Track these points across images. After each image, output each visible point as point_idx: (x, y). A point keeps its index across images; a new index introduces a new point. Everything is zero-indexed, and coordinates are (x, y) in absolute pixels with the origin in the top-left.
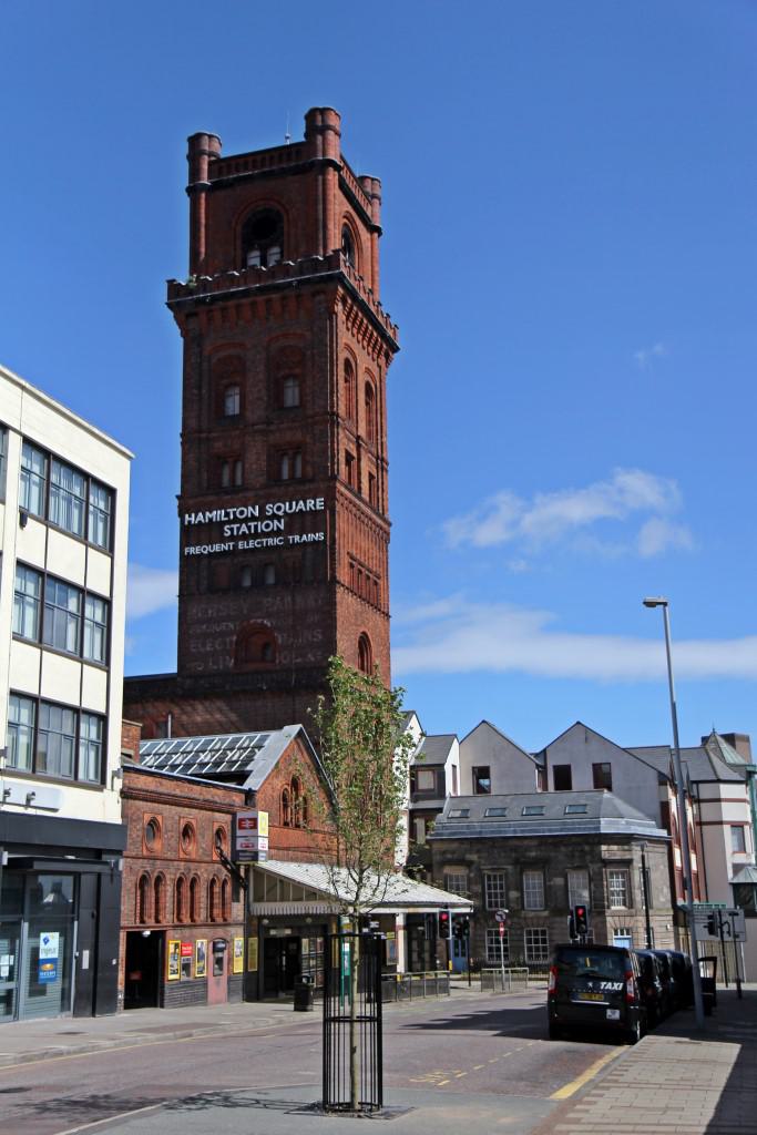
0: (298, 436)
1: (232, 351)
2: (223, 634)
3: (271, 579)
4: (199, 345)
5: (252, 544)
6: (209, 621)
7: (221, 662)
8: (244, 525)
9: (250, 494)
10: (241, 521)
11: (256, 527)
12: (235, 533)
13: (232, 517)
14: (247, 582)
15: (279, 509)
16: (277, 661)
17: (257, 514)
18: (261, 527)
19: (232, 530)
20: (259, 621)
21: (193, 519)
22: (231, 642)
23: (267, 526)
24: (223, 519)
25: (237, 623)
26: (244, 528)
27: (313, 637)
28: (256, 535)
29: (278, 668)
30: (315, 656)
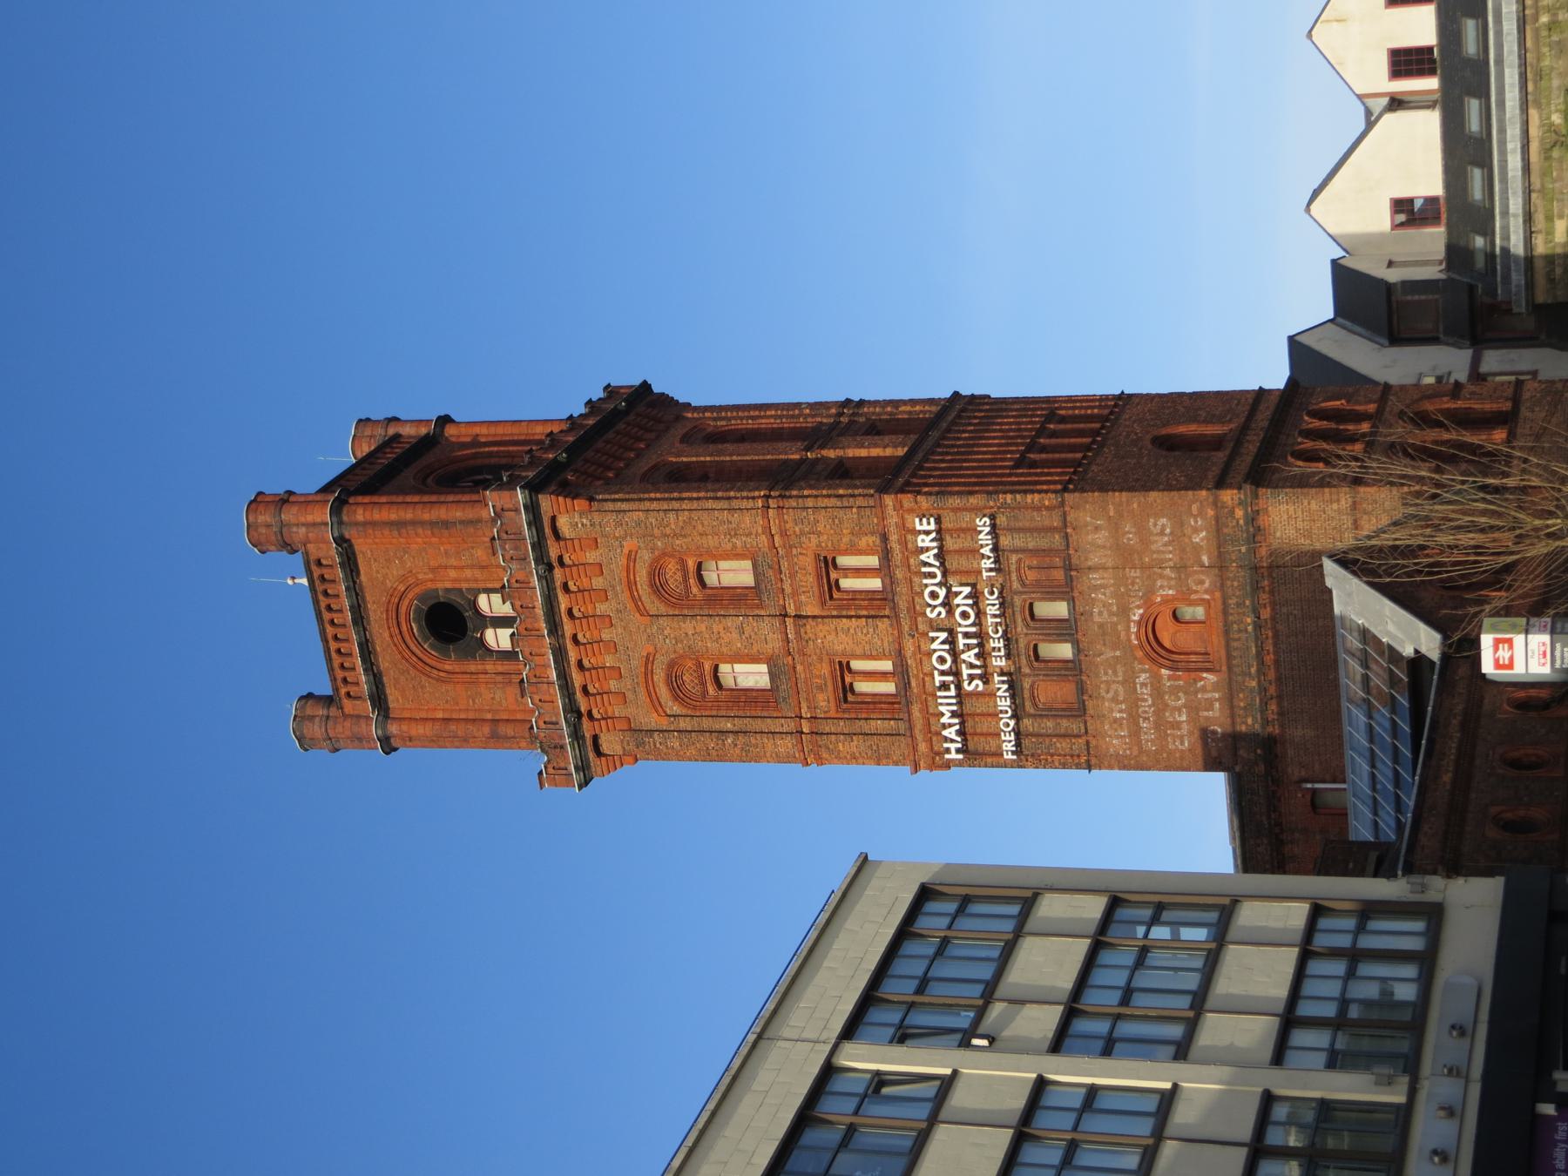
0: (808, 562)
1: (659, 677)
2: (1158, 693)
3: (1060, 609)
5: (996, 643)
6: (1134, 718)
7: (1209, 695)
8: (964, 656)
9: (909, 646)
10: (955, 654)
11: (966, 635)
12: (978, 671)
13: (950, 678)
14: (1065, 650)
15: (934, 595)
16: (1207, 597)
17: (943, 635)
18: (965, 626)
19: (972, 678)
20: (1134, 629)
21: (953, 746)
22: (1170, 677)
23: (965, 615)
24: (953, 692)
25: (1138, 667)
26: (969, 656)
28: (981, 636)
29: (1218, 594)
30: (1196, 530)
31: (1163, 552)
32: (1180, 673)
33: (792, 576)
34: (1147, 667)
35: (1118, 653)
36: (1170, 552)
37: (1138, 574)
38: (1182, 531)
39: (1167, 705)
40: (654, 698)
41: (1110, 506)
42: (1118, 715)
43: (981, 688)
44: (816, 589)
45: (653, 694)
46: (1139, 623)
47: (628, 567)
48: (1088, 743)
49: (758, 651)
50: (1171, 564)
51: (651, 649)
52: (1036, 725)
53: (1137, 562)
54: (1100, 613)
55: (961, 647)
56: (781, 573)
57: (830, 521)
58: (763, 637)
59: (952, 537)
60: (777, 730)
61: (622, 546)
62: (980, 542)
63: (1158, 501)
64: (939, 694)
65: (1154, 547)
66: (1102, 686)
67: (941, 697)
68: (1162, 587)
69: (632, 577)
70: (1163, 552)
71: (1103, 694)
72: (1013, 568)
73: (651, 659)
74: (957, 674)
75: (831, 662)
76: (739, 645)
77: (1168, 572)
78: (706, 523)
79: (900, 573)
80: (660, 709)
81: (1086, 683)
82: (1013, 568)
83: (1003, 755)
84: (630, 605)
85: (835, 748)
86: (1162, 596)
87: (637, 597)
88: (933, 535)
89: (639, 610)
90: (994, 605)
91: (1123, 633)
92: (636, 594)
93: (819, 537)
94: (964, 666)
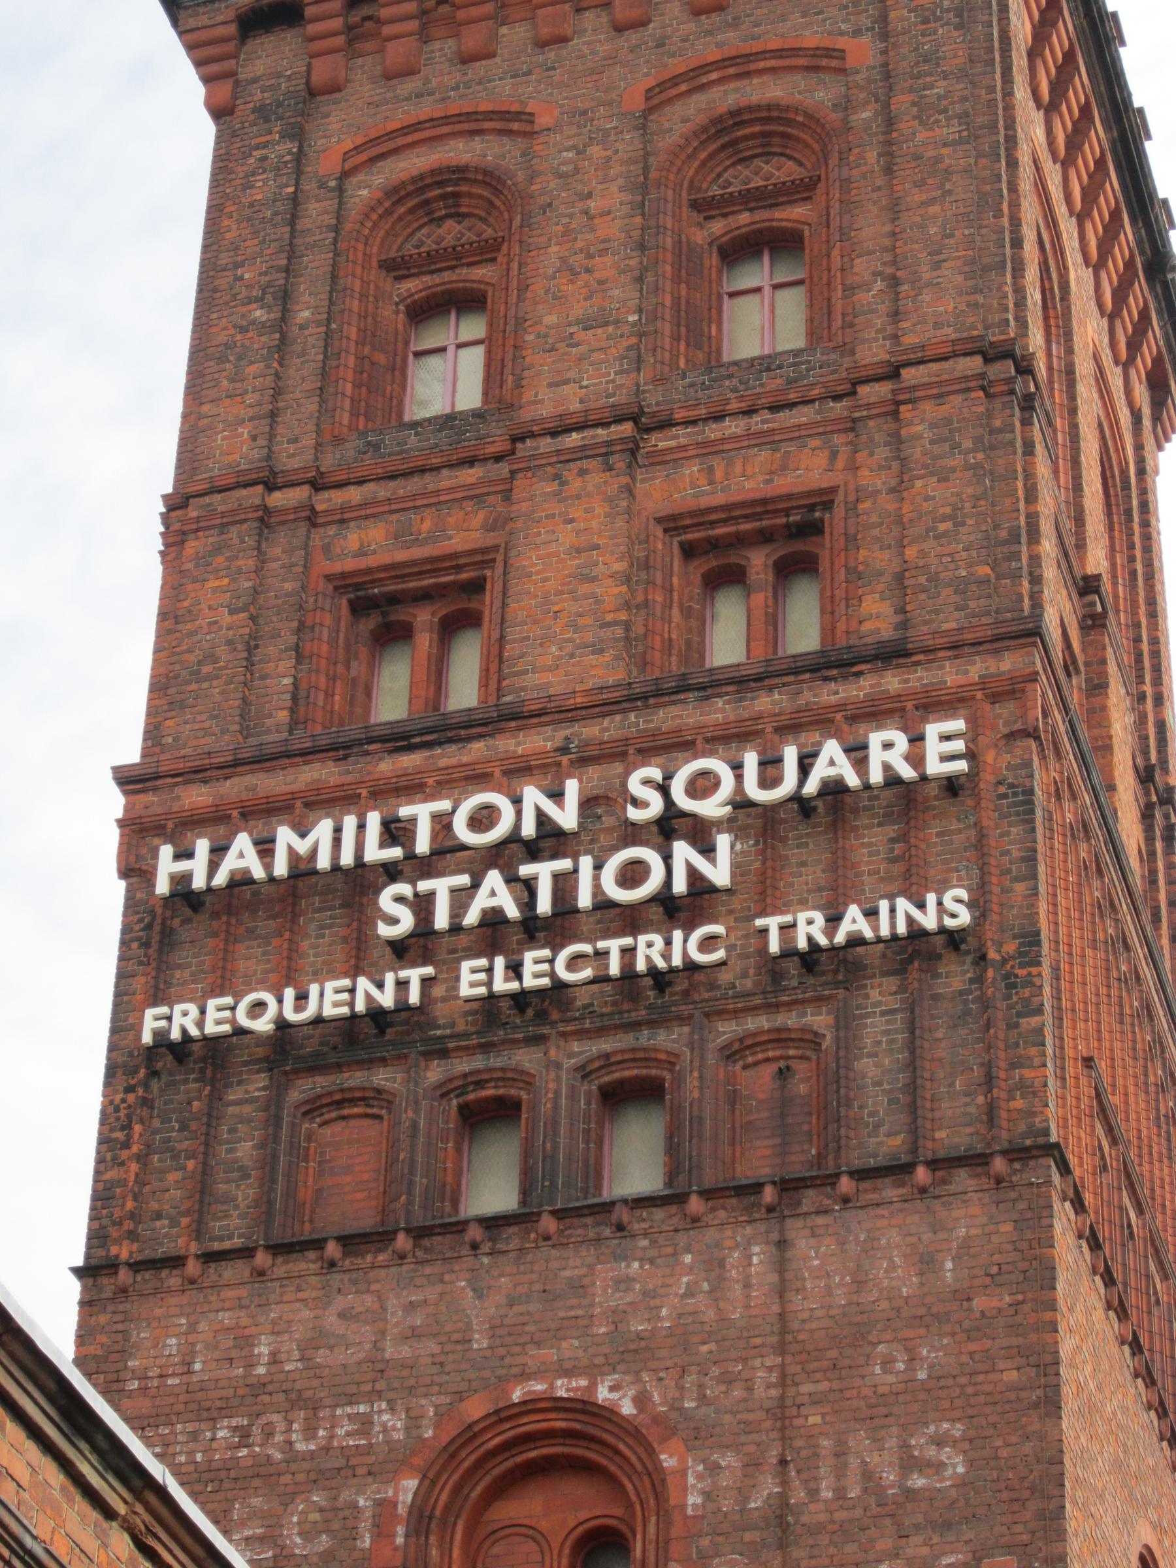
4: (298, 134)
8: (494, 878)
12: (441, 921)
15: (702, 785)
19: (423, 905)
21: (198, 867)
22: (385, 1507)
24: (374, 853)
27: (910, 1463)
31: (840, 1471)
32: (400, 1540)
33: (765, 439)
34: (429, 1433)
35: (480, 1341)
36: (840, 1493)
37: (759, 1391)
38: (918, 1528)
39: (288, 1499)
40: (400, 142)
41: (1007, 1299)
42: (263, 1350)
43: (385, 931)
44: (720, 499)
45: (409, 139)
46: (584, 1407)
47: (795, 51)
48: (175, 1262)
49: (531, 367)
50: (798, 1495)
51: (543, 121)
52: (247, 1109)
53: (805, 1388)
54: (622, 1283)
55: (525, 870)
56: (774, 408)
57: (948, 510)
58: (571, 375)
59: (892, 841)
60: (280, 430)
61: (857, 33)
62: (884, 905)
63: (1028, 1448)
64: (374, 819)
65: (859, 1441)
66: (369, 1299)
67: (361, 827)
68: (714, 1469)
69: (762, 65)
70: (840, 1471)
71: (340, 1302)
72: (790, 1020)
73: (515, 126)
74: (426, 867)
75: (484, 557)
76: (551, 319)
77: (769, 1486)
78: (935, 209)
79: (774, 703)
80: (364, 157)
81: (380, 1250)
82: (790, 1020)
83: (155, 1004)
84: (676, 65)
85: (217, 571)
86: (683, 1473)
87: (704, 80)
88: (907, 772)
89: (663, 86)
90: (666, 956)
91: (549, 1354)
92: (714, 76)
93: (892, 491)
94: (464, 880)
